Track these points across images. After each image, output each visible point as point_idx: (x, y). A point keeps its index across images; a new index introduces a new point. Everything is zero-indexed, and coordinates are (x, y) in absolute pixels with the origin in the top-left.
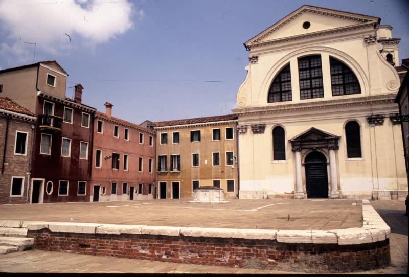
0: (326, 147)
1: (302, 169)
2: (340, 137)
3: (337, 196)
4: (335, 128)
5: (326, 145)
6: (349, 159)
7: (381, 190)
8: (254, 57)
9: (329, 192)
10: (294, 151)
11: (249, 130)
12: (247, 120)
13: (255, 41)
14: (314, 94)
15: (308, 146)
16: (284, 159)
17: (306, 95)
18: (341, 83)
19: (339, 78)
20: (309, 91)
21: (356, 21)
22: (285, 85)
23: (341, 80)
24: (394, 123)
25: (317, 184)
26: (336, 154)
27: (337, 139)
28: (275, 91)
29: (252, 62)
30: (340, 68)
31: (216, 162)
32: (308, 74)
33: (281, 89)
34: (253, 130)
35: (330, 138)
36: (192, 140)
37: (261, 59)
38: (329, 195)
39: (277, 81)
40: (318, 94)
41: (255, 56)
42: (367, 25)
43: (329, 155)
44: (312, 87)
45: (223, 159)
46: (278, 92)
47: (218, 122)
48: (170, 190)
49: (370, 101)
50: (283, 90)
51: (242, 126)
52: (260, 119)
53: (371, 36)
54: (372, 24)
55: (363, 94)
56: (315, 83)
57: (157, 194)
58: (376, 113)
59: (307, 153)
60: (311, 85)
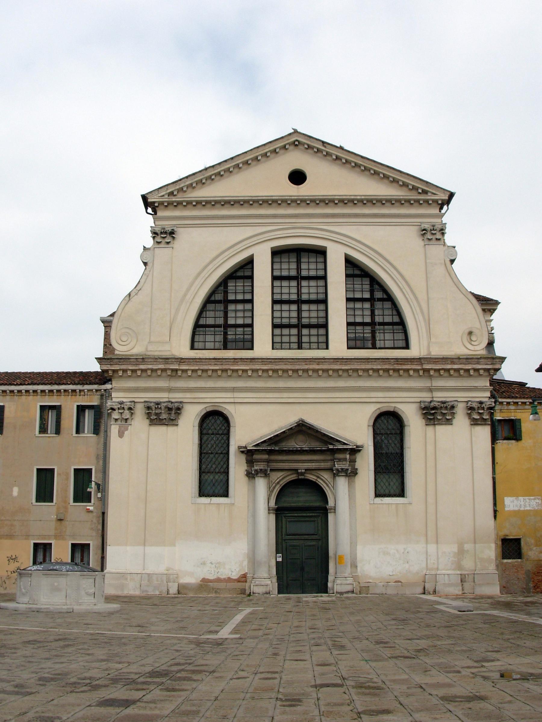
0: (331, 470)
1: (268, 521)
2: (362, 447)
3: (349, 588)
4: (350, 421)
5: (328, 465)
6: (378, 500)
7: (444, 572)
8: (166, 233)
9: (331, 578)
10: (251, 475)
11: (140, 410)
13: (171, 194)
14: (305, 339)
16: (226, 494)
17: (286, 339)
18: (368, 320)
19: (363, 309)
20: (294, 331)
21: (405, 188)
22: (236, 311)
23: (368, 312)
24: (475, 423)
25: (304, 556)
26: (351, 485)
27: (355, 451)
28: (210, 321)
29: (159, 243)
30: (367, 287)
31: (45, 492)
32: (294, 290)
33: (226, 317)
34: (149, 414)
35: (340, 447)
38: (330, 585)
39: (219, 297)
41: (169, 229)
42: (426, 201)
44: (301, 323)
45: (64, 485)
46: (219, 326)
47: (56, 387)
50: (231, 321)
51: (121, 403)
52: (170, 390)
53: (433, 226)
54: (435, 201)
55: (414, 351)
56: (310, 314)
58: (440, 396)
59: (283, 483)
60: (299, 318)
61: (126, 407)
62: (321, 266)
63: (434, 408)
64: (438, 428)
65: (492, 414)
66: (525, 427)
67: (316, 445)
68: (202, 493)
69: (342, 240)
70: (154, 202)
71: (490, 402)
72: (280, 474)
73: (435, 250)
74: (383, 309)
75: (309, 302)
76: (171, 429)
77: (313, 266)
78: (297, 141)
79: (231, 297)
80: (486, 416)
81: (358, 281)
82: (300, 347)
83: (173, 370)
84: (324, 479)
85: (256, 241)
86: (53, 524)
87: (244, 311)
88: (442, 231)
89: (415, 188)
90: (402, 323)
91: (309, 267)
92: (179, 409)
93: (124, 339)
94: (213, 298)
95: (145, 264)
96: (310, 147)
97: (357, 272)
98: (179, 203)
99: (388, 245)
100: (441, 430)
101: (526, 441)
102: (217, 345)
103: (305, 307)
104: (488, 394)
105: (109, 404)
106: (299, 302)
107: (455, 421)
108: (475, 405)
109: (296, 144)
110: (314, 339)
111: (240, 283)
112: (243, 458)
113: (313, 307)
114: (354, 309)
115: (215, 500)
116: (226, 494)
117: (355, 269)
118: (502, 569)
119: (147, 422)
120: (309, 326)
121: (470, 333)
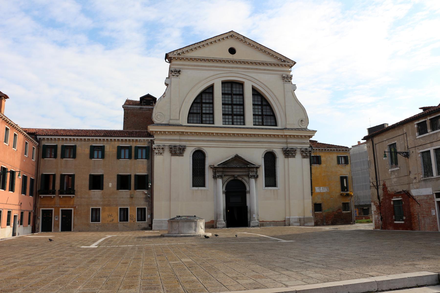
3: (257, 224)
4: (255, 155)
6: (267, 188)
8: (176, 71)
10: (215, 177)
12: (166, 140)
13: (179, 54)
14: (235, 120)
15: (230, 174)
18: (260, 113)
19: (258, 109)
20: (230, 117)
21: (276, 59)
22: (206, 107)
23: (260, 110)
24: (304, 157)
28: (195, 111)
30: (260, 99)
33: (202, 110)
34: (171, 152)
36: (119, 157)
37: (183, 73)
39: (198, 101)
40: (257, 120)
41: (178, 70)
43: (249, 183)
46: (199, 113)
48: (57, 219)
50: (204, 112)
51: (159, 146)
52: (180, 140)
56: (237, 110)
57: (37, 226)
58: (290, 146)
60: (232, 111)
61: (161, 148)
62: (241, 90)
63: (288, 151)
64: (289, 159)
65: (310, 154)
66: (323, 159)
68: (194, 186)
69: (251, 79)
70: (171, 57)
71: (310, 149)
72: (227, 177)
73: (287, 85)
74: (266, 109)
75: (236, 105)
76: (181, 157)
77: (238, 89)
78: (232, 35)
79: (204, 101)
81: (256, 97)
82: (233, 124)
83: (181, 132)
84: (245, 180)
85: (215, 77)
87: (209, 107)
88: (291, 77)
89: (280, 59)
90: (273, 116)
91: (236, 90)
93: (159, 117)
94: (196, 101)
95: (167, 85)
96: (238, 38)
97: (255, 93)
98: (183, 58)
99: (268, 82)
100: (291, 159)
101: (323, 165)
102: (198, 121)
103: (235, 107)
104: (309, 146)
105: (154, 146)
106: (232, 104)
107: (296, 156)
108: (304, 150)
109: (231, 36)
110: (239, 120)
111: (207, 95)
112: (211, 170)
113: (238, 107)
116: (204, 186)
117: (256, 93)
118: (315, 215)
119: (170, 154)
120: (237, 115)
121: (302, 121)
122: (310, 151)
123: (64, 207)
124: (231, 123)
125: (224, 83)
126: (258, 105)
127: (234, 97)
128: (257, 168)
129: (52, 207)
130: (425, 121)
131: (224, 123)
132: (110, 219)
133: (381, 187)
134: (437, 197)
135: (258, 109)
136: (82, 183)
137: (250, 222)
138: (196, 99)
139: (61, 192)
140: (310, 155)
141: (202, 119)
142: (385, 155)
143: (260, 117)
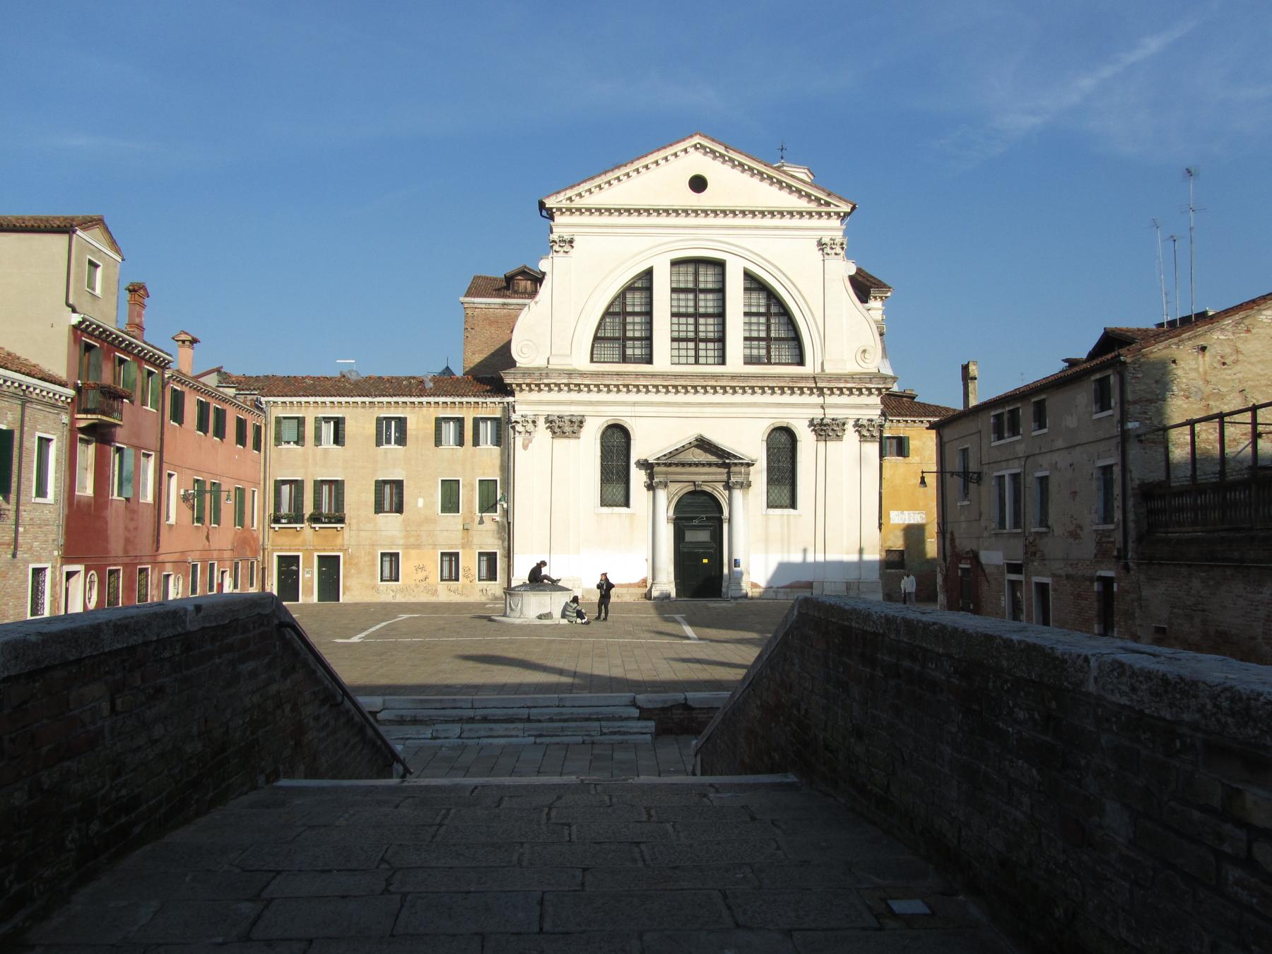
4: (744, 434)
10: (650, 487)
14: (702, 353)
15: (684, 478)
17: (683, 353)
18: (763, 334)
22: (634, 323)
23: (763, 328)
30: (763, 302)
31: (451, 502)
33: (625, 330)
38: (724, 590)
41: (567, 238)
45: (470, 497)
46: (617, 339)
49: (819, 386)
50: (629, 334)
54: (838, 214)
55: (807, 369)
58: (831, 413)
59: (680, 494)
60: (696, 331)
65: (881, 432)
67: (713, 459)
68: (604, 503)
76: (572, 442)
79: (629, 309)
80: (876, 434)
81: (754, 295)
82: (697, 362)
86: (460, 534)
92: (581, 422)
93: (525, 350)
101: (914, 458)
103: (702, 321)
106: (696, 315)
108: (865, 422)
114: (750, 324)
115: (616, 509)
116: (627, 504)
117: (754, 283)
121: (864, 351)
122: (881, 426)
123: (324, 550)
124: (692, 360)
125: (675, 263)
126: (758, 314)
127: (702, 296)
128: (749, 465)
129: (298, 550)
130: (1002, 414)
131: (676, 360)
132: (421, 575)
133: (948, 536)
134: (1009, 572)
135: (759, 324)
136: (358, 499)
137: (728, 587)
138: (611, 304)
139: (315, 519)
140: (881, 437)
141: (624, 352)
142: (923, 478)
143: (763, 344)
